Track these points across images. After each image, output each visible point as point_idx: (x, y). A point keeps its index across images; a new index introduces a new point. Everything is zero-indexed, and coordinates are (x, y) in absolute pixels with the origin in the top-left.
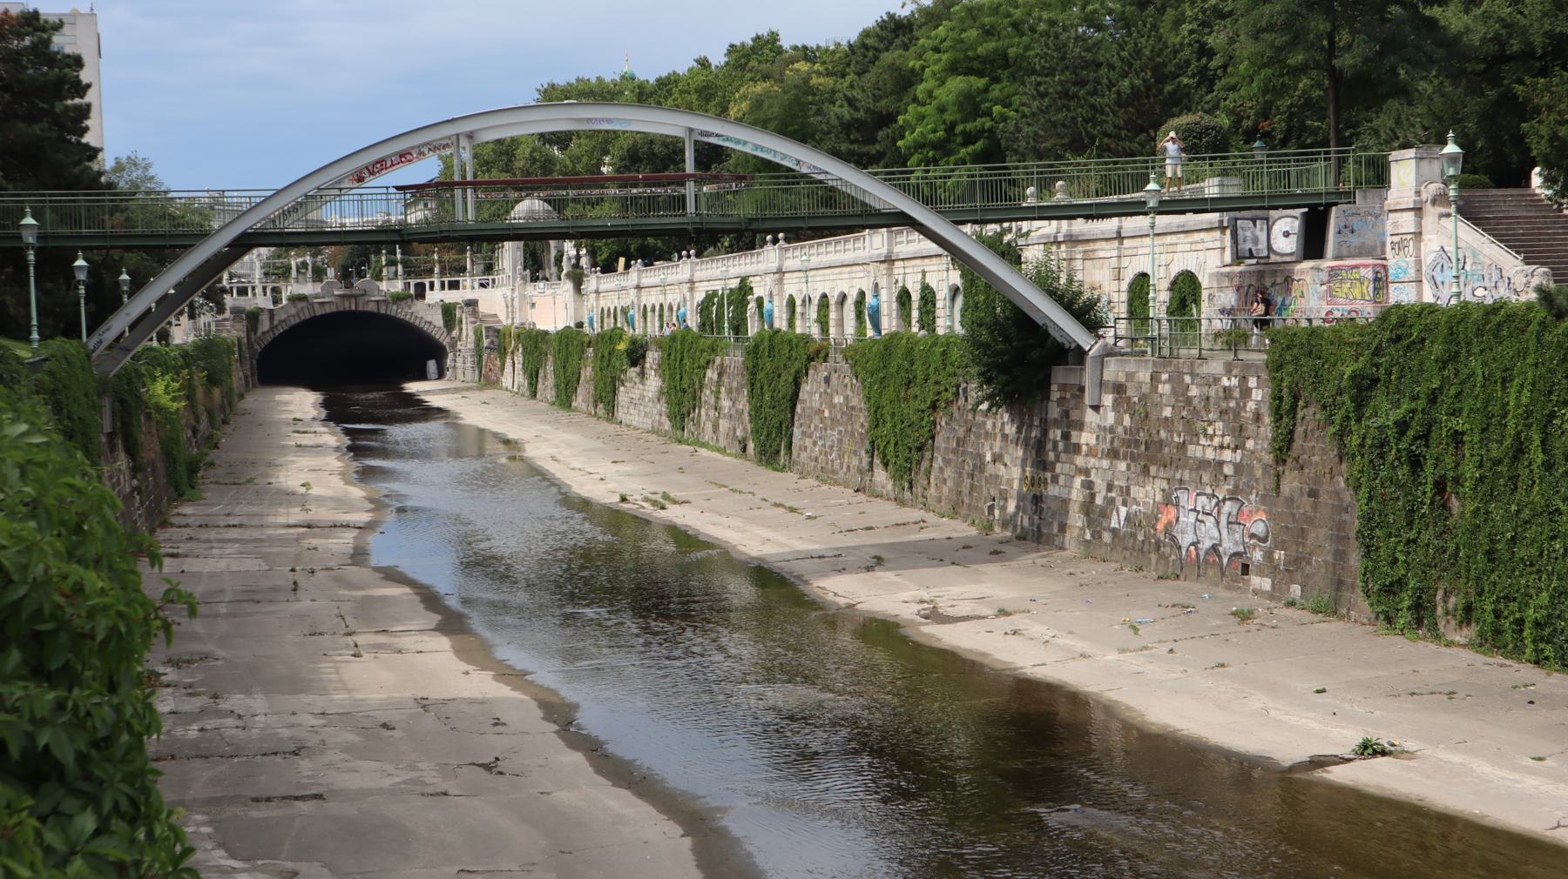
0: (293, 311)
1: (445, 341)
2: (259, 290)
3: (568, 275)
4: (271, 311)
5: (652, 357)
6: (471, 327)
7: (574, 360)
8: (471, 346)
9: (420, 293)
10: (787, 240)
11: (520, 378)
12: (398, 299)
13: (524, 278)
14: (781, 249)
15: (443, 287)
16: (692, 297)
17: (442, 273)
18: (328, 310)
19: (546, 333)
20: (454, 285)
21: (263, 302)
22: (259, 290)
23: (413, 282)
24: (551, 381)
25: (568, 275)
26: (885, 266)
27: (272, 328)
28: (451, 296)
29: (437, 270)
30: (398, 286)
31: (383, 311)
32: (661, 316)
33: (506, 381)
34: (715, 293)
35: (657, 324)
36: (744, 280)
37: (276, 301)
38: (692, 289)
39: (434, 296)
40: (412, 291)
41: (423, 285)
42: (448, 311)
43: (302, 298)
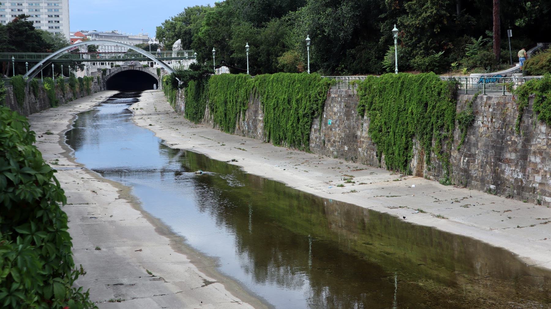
1: (157, 79)
9: (152, 66)
12: (145, 66)
18: (125, 69)
23: (150, 62)
27: (110, 74)
37: (112, 67)
42: (158, 70)
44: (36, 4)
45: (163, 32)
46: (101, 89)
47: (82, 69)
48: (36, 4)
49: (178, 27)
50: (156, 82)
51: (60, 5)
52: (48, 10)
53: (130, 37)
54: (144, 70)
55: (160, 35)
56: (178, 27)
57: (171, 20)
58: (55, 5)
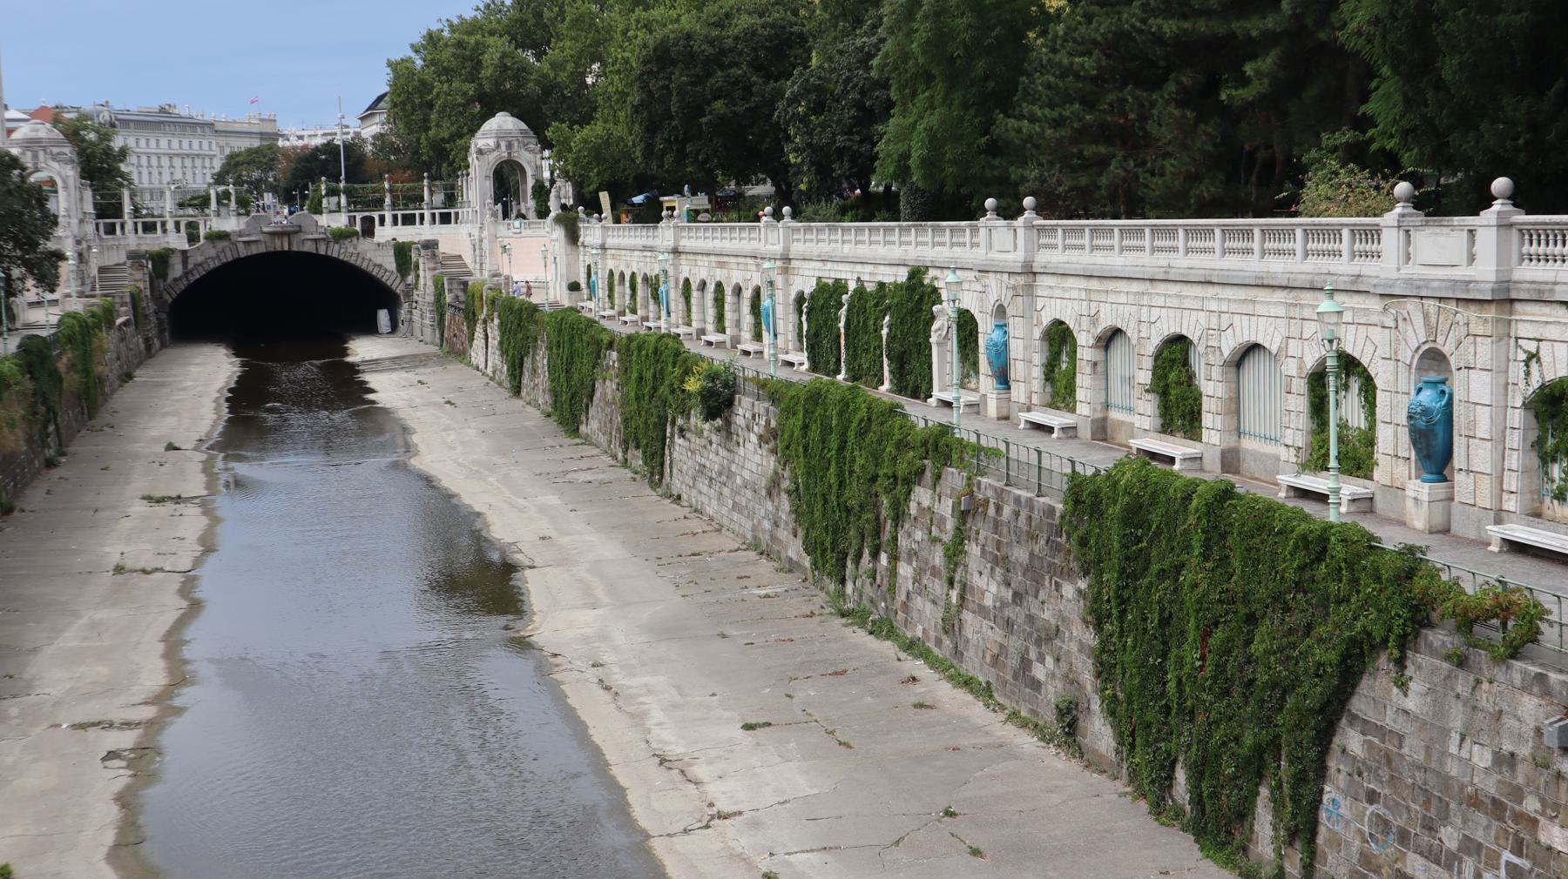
0: (212, 252)
1: (399, 289)
2: (170, 226)
3: (558, 220)
4: (184, 252)
5: (745, 408)
6: (429, 275)
7: (583, 365)
8: (430, 299)
9: (368, 231)
10: (1043, 210)
11: (495, 359)
12: (340, 236)
13: (494, 215)
14: (1029, 226)
15: (395, 222)
16: (787, 283)
17: (394, 206)
18: (254, 250)
19: (535, 309)
20: (409, 220)
21: (178, 241)
22: (170, 226)
23: (359, 216)
24: (543, 378)
25: (558, 220)
26: (1491, 313)
27: (186, 274)
28: (405, 234)
29: (388, 200)
30: (340, 221)
32: (719, 301)
33: (477, 354)
34: (840, 286)
35: (711, 313)
36: (916, 273)
37: (193, 238)
38: (785, 271)
39: (387, 233)
40: (358, 228)
41: (372, 219)
42: (402, 252)
43: (223, 236)
45: (423, 82)
46: (149, 347)
47: (48, 281)
49: (491, 57)
50: (390, 300)
53: (219, 127)
54: (335, 251)
55: (410, 96)
56: (491, 57)
57: (446, 34)
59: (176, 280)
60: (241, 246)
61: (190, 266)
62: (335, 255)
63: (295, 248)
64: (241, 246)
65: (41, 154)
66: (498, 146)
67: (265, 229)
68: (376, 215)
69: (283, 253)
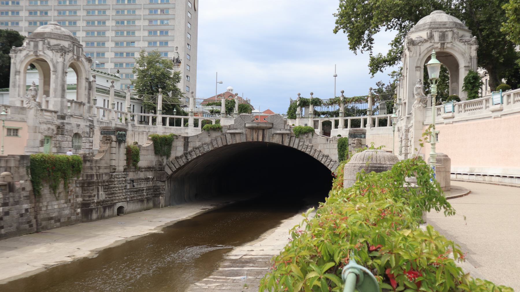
0: (208, 140)
2: (191, 122)
9: (326, 132)
15: (346, 126)
18: (238, 140)
22: (191, 122)
27: (185, 154)
31: (286, 144)
44: (128, 21)
48: (128, 21)
51: (171, 23)
52: (150, 32)
54: (296, 144)
58: (162, 21)
59: (177, 158)
60: (229, 137)
61: (190, 149)
62: (295, 147)
63: (267, 140)
64: (229, 137)
65: (40, 44)
66: (431, 37)
67: (247, 125)
68: (332, 120)
69: (258, 142)
